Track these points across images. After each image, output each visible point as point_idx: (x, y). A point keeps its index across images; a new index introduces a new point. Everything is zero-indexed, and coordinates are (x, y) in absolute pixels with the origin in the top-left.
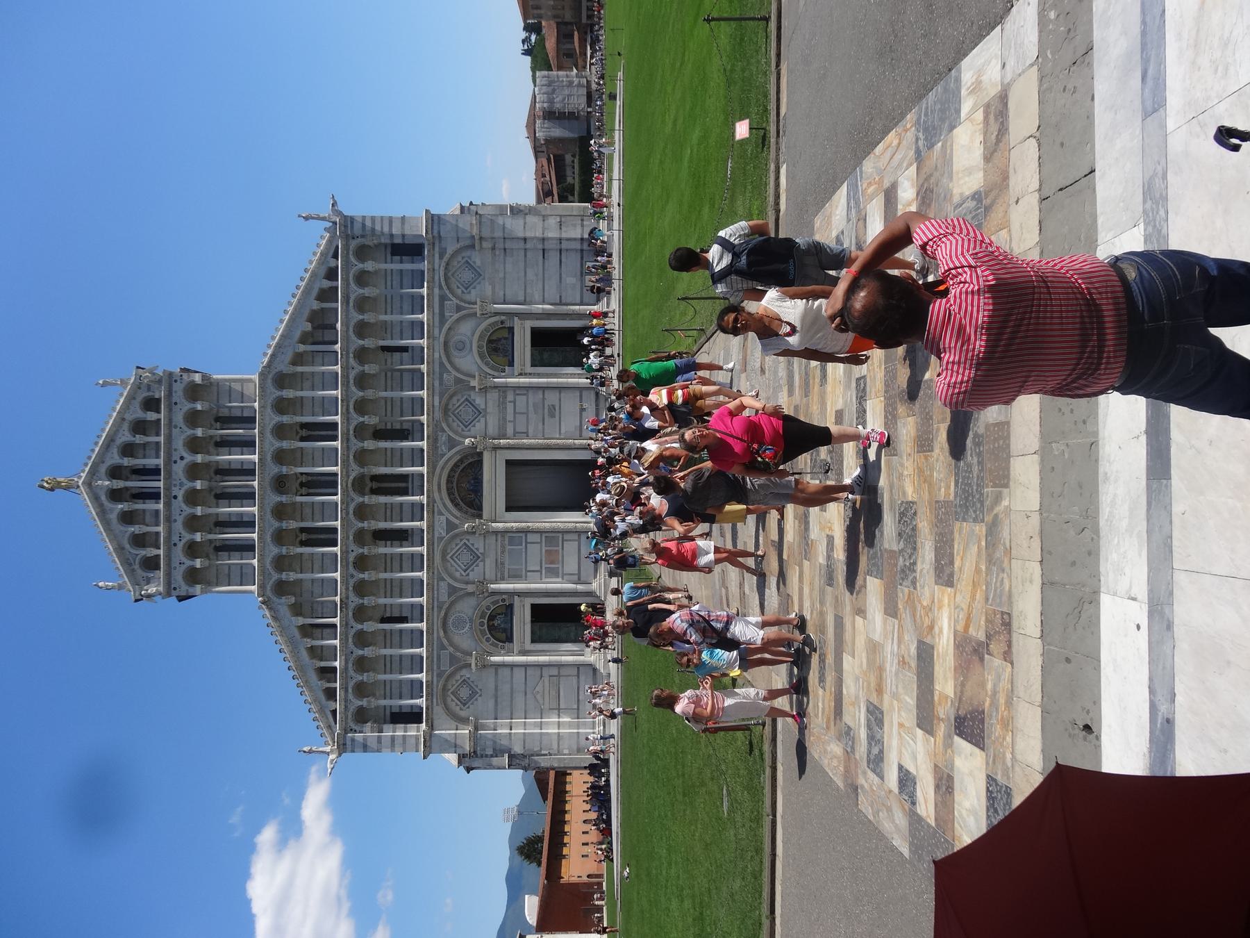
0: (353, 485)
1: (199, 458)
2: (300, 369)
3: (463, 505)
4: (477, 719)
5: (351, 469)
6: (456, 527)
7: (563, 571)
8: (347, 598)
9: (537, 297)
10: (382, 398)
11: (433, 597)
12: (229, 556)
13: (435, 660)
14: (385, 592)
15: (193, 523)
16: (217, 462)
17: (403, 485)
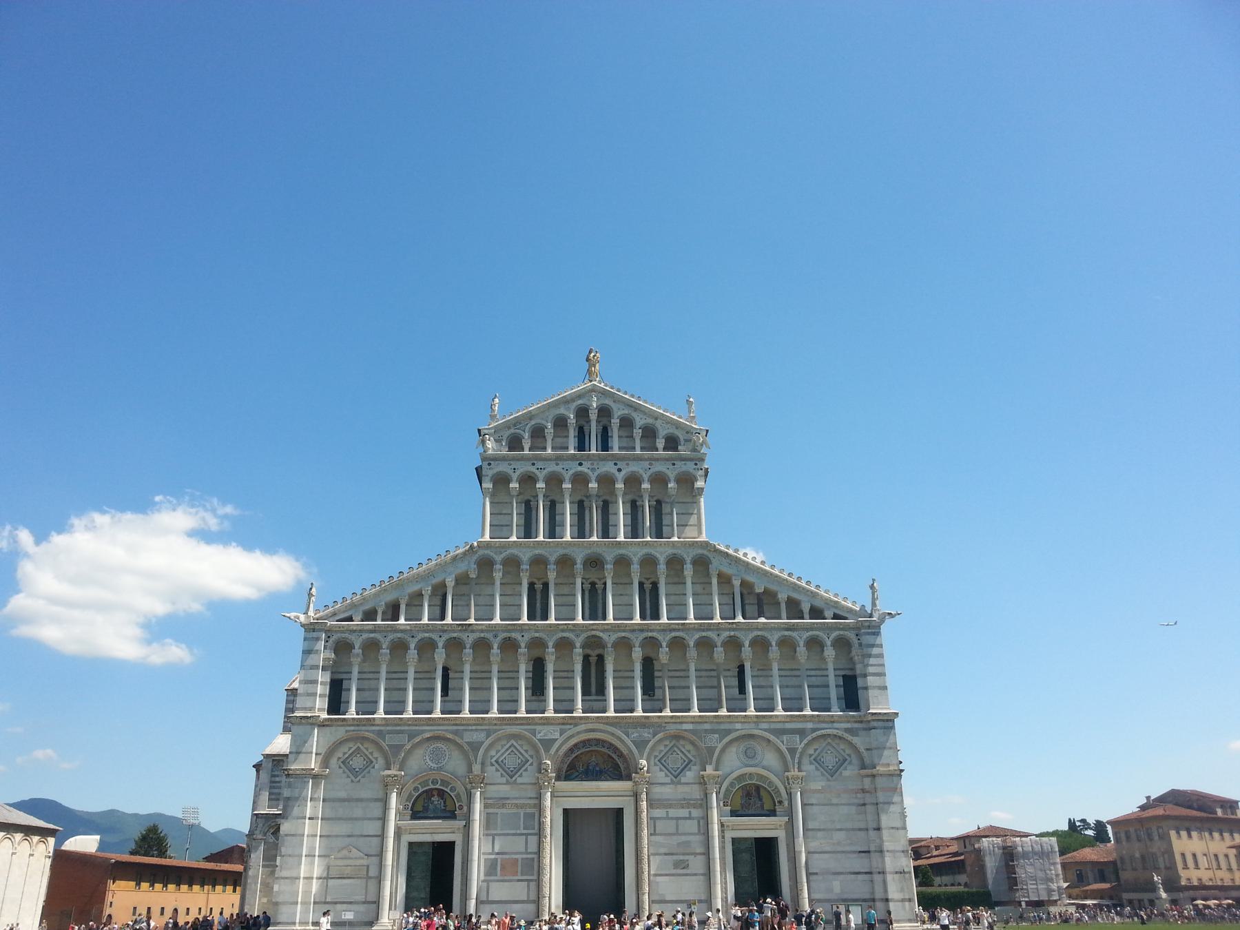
0: (594, 636)
1: (620, 486)
2: (715, 581)
3: (571, 759)
4: (325, 777)
6: (547, 750)
7: (491, 881)
8: (473, 631)
9: (814, 845)
10: (688, 666)
11: (468, 725)
12: (520, 514)
13: (398, 728)
14: (476, 672)
15: (554, 481)
16: (616, 502)
17: (593, 689)
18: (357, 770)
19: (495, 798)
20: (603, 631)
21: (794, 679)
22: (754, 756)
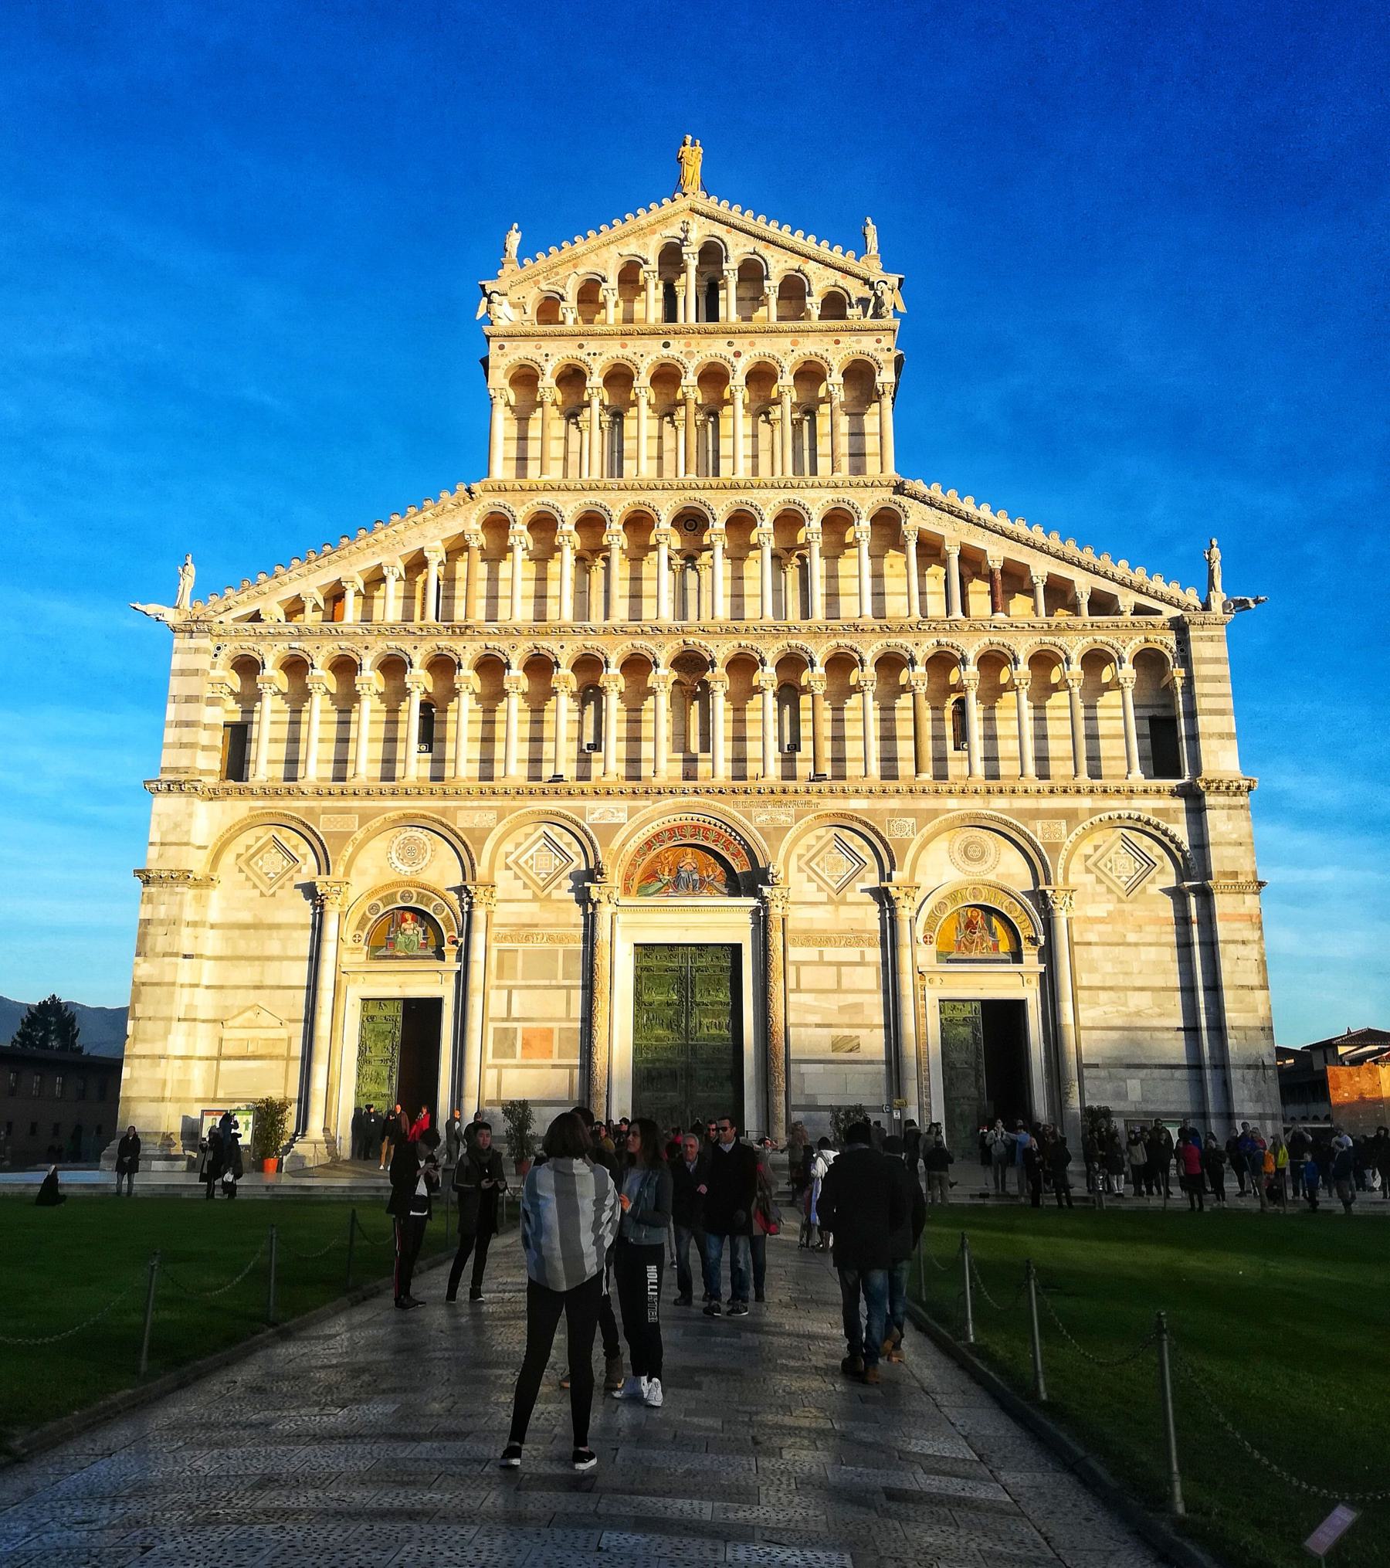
1: (738, 380)
6: (606, 843)
7: (506, 1066)
18: (271, 875)
19: (515, 925)
21: (1057, 722)
22: (980, 858)
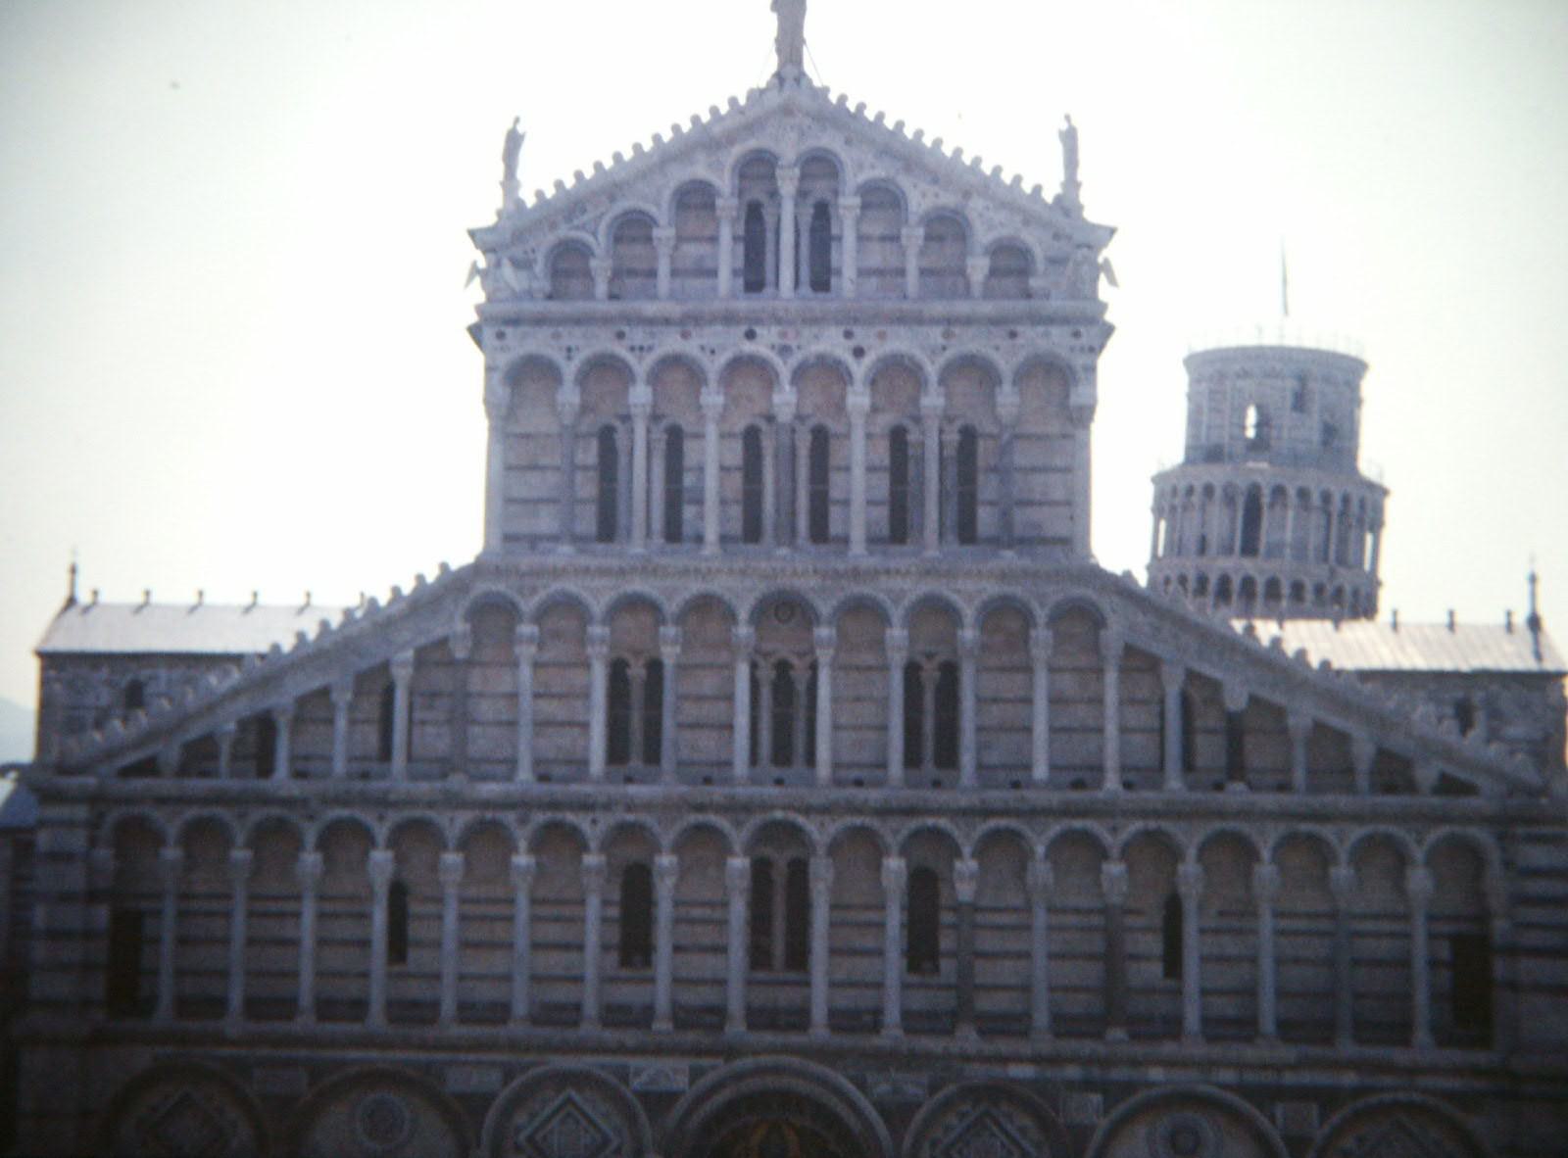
2: (1111, 677)
5: (827, 819)
14: (477, 901)
20: (808, 810)
